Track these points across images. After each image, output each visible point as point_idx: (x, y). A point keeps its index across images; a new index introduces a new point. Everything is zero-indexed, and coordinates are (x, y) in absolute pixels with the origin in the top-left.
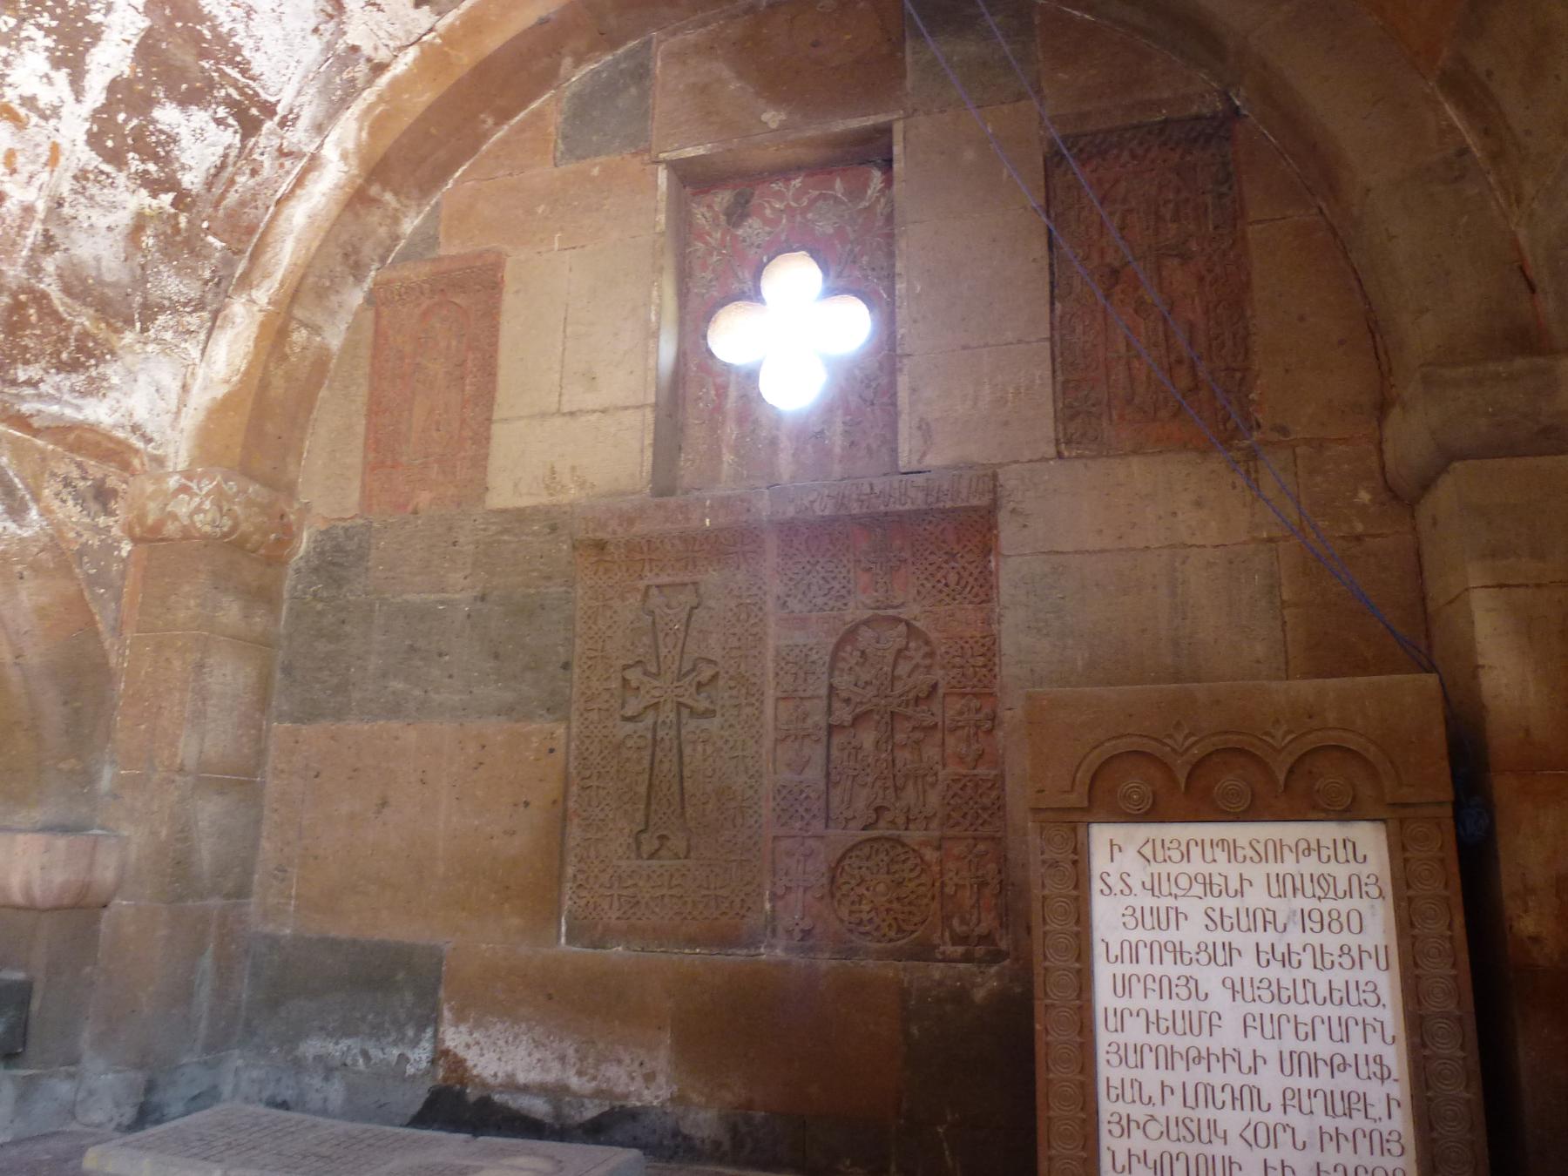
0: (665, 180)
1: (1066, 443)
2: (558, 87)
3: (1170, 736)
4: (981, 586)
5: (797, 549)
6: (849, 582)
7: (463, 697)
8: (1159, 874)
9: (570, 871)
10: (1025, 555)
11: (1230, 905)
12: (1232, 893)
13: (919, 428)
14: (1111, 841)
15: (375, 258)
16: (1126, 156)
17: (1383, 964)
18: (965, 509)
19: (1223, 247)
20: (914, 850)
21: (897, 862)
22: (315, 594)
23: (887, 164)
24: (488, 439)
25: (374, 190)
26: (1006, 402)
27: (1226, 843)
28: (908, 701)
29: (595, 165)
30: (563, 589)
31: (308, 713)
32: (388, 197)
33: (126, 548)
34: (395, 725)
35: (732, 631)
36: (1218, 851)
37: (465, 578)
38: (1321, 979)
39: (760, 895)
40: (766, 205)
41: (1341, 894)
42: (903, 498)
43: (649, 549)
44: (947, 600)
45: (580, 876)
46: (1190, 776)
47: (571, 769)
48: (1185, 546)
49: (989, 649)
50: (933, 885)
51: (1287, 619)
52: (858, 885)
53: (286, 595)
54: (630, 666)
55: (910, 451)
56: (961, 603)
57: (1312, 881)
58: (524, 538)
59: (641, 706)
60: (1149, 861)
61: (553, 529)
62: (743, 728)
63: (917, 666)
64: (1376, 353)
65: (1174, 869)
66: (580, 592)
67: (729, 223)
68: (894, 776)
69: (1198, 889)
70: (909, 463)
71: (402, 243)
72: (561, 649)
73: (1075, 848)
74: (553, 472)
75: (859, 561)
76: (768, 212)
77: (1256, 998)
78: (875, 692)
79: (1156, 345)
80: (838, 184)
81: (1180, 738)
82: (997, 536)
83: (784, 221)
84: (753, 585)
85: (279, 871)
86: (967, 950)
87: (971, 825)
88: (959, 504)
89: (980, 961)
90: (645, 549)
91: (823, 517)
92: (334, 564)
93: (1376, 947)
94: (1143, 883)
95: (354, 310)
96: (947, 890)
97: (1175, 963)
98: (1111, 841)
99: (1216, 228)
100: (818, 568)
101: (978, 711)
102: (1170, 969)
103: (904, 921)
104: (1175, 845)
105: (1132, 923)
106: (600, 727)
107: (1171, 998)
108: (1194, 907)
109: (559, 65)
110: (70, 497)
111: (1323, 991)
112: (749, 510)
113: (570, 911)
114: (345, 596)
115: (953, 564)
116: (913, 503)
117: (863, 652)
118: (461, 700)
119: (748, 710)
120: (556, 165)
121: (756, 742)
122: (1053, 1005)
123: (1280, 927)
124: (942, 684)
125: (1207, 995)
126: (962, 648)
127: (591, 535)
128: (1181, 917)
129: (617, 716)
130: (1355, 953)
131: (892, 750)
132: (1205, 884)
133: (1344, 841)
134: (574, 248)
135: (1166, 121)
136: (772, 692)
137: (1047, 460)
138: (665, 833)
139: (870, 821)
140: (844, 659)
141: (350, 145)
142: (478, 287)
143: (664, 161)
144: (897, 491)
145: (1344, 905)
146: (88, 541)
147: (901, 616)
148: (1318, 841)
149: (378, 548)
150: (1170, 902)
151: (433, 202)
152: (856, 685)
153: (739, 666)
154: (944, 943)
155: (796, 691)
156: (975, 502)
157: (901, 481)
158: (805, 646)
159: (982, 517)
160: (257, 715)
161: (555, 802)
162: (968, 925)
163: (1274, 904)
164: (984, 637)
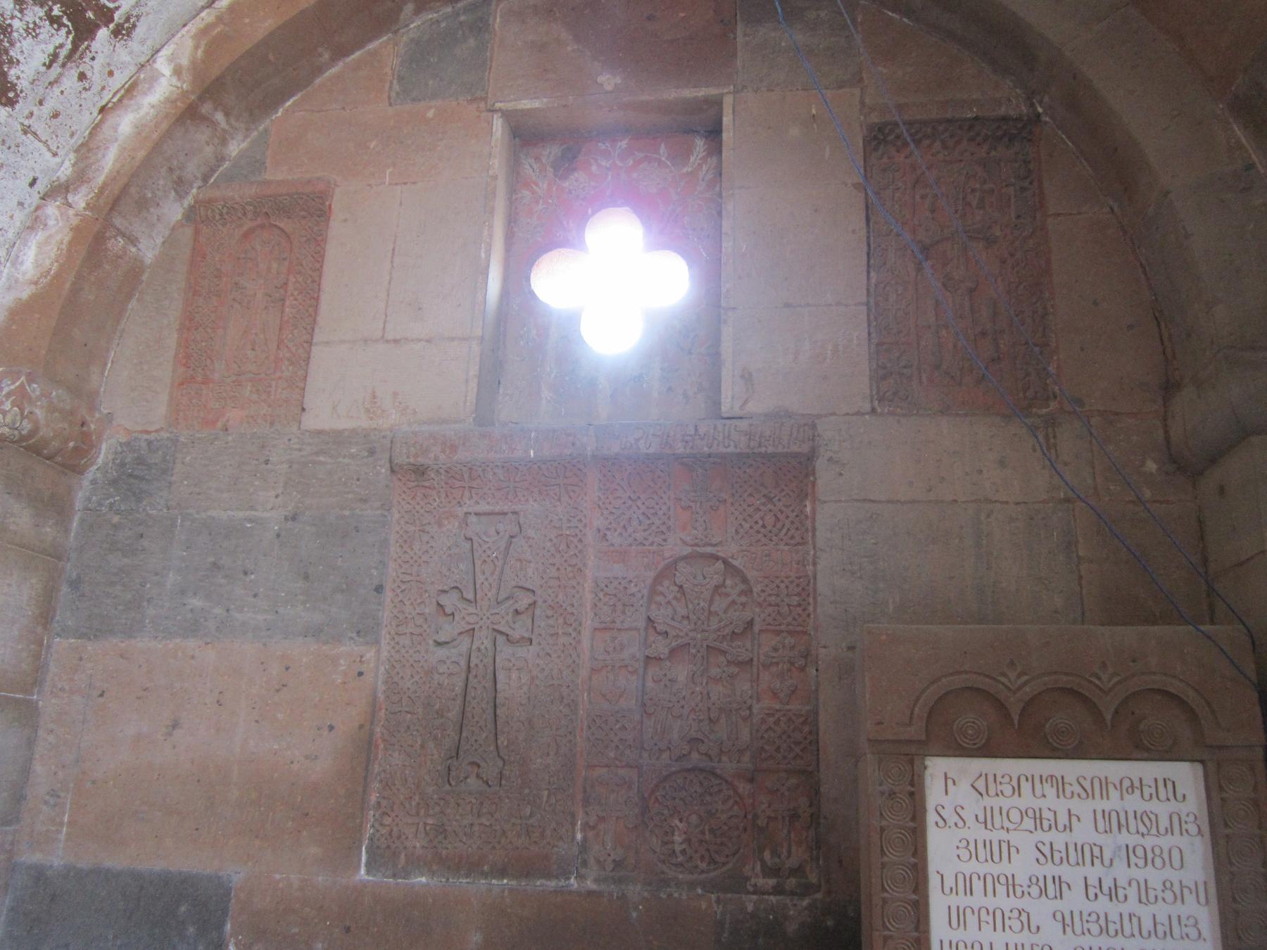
0: (500, 129)
1: (879, 401)
2: (396, 32)
3: (1004, 675)
4: (797, 529)
5: (618, 484)
6: (669, 518)
7: (268, 617)
8: (992, 808)
9: (373, 798)
10: (840, 501)
11: (1059, 839)
12: (1061, 827)
13: (742, 376)
14: (946, 774)
15: (199, 175)
16: (938, 144)
17: (1202, 899)
19: (1026, 233)
20: (726, 781)
21: (711, 795)
22: (111, 506)
23: (714, 133)
24: (307, 360)
25: (206, 108)
27: (1054, 778)
28: (724, 636)
29: (431, 107)
30: (379, 512)
31: (96, 629)
32: (219, 117)
34: (192, 644)
35: (551, 561)
36: (1047, 786)
37: (277, 496)
38: (1145, 913)
39: (573, 824)
40: (592, 161)
41: (1162, 830)
42: (726, 441)
43: (470, 477)
44: (763, 540)
45: (384, 803)
46: (1021, 715)
47: (381, 697)
48: (991, 502)
49: (803, 589)
50: (745, 816)
51: (1083, 573)
52: (671, 816)
53: (78, 505)
54: (444, 592)
55: (733, 398)
56: (777, 544)
57: (1135, 818)
58: (341, 459)
59: (456, 632)
60: (981, 794)
61: (372, 452)
62: (559, 657)
63: (734, 602)
64: (1161, 339)
65: (1005, 803)
66: (397, 516)
67: (556, 176)
68: (709, 709)
69: (1028, 823)
70: (732, 408)
71: (227, 164)
72: (375, 573)
73: (912, 780)
74: (374, 397)
75: (680, 499)
76: (594, 168)
77: (1086, 931)
78: (693, 626)
80: (663, 149)
81: (1012, 675)
83: (610, 177)
84: (574, 517)
85: (52, 795)
86: (778, 883)
87: (784, 758)
88: (780, 450)
89: (792, 893)
90: (466, 476)
91: (647, 454)
92: (136, 477)
93: (1196, 884)
94: (977, 816)
95: (172, 224)
96: (759, 822)
97: (1008, 896)
98: (946, 774)
99: (1018, 217)
100: (639, 503)
101: (792, 648)
102: (1003, 901)
103: (716, 852)
104: (1007, 779)
105: (965, 854)
106: (411, 651)
107: (1004, 930)
108: (1024, 840)
109: (401, 9)
111: (1147, 925)
112: (573, 444)
113: (371, 839)
114: (144, 510)
115: (770, 506)
116: (736, 447)
117: (681, 587)
118: (265, 620)
119: (563, 640)
120: (390, 105)
121: (573, 671)
122: (891, 937)
123: (1107, 862)
124: (757, 620)
125: (1038, 928)
126: (778, 587)
127: (412, 460)
128: (1013, 850)
129: (431, 642)
130: (1177, 888)
131: (707, 683)
132: (1035, 818)
133: (1165, 780)
134: (405, 183)
135: (976, 118)
136: (589, 622)
137: (863, 414)
138: (476, 760)
139: (684, 752)
140: (663, 594)
141: (185, 62)
142: (302, 213)
143: (500, 110)
144: (721, 435)
145: (1165, 842)
147: (720, 554)
148: (1141, 780)
149: (183, 463)
150: (1003, 835)
151: (261, 128)
152: (673, 619)
153: (557, 597)
154: (757, 876)
155: (614, 622)
156: (795, 448)
157: (725, 425)
158: (624, 578)
159: (800, 463)
160: (39, 629)
161: (361, 727)
162: (779, 857)
163: (1101, 839)
164: (799, 578)
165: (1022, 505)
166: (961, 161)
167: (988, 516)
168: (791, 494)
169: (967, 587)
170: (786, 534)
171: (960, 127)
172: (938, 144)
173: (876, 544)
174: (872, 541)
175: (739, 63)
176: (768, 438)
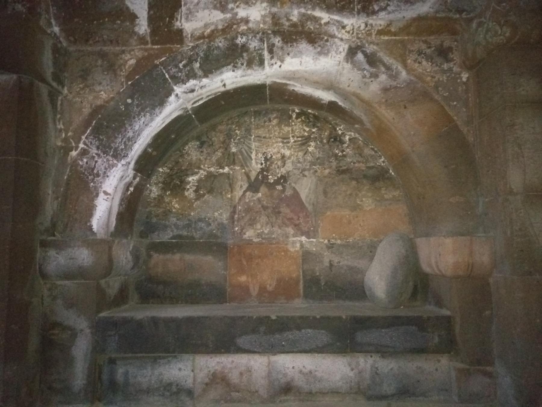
33: (465, 76)
110: (423, 60)
146: (439, 79)
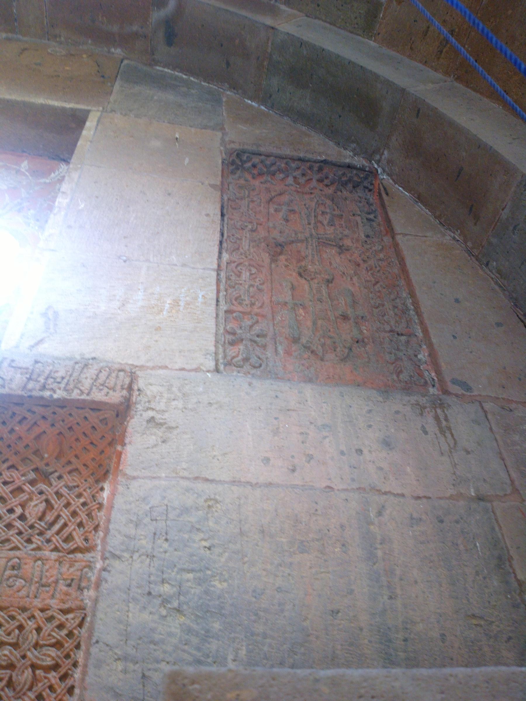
1: (225, 365)
4: (80, 525)
10: (159, 478)
16: (290, 180)
18: (81, 405)
19: (376, 248)
26: (161, 311)
44: (16, 540)
49: (70, 635)
56: (38, 548)
70: (17, 347)
79: (320, 301)
82: (119, 455)
88: (75, 395)
115: (42, 486)
156: (98, 396)
159: (104, 421)
164: (65, 612)
165: (425, 500)
166: (311, 193)
167: (380, 514)
168: (81, 468)
169: (361, 629)
170: (58, 533)
171: (310, 168)
172: (290, 180)
173: (209, 549)
174: (204, 544)
175: (112, 98)
176: (59, 380)
